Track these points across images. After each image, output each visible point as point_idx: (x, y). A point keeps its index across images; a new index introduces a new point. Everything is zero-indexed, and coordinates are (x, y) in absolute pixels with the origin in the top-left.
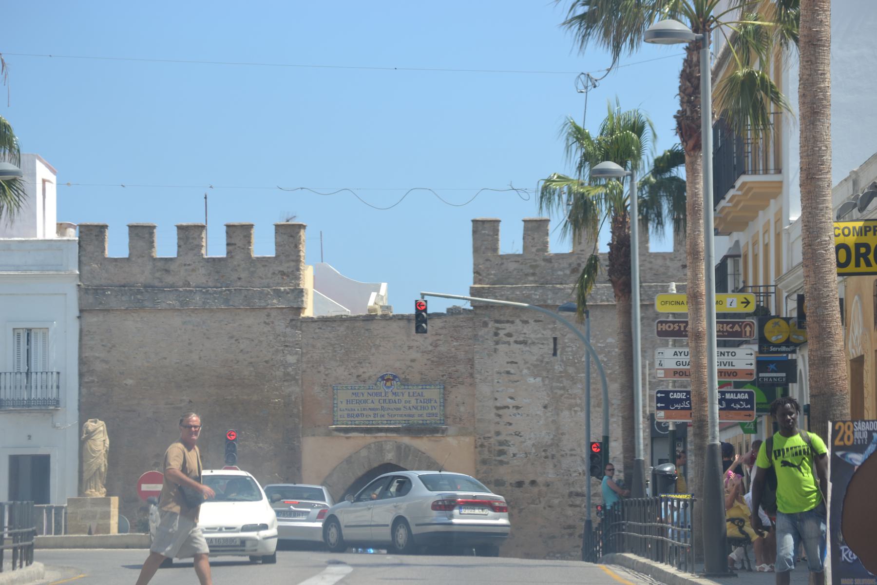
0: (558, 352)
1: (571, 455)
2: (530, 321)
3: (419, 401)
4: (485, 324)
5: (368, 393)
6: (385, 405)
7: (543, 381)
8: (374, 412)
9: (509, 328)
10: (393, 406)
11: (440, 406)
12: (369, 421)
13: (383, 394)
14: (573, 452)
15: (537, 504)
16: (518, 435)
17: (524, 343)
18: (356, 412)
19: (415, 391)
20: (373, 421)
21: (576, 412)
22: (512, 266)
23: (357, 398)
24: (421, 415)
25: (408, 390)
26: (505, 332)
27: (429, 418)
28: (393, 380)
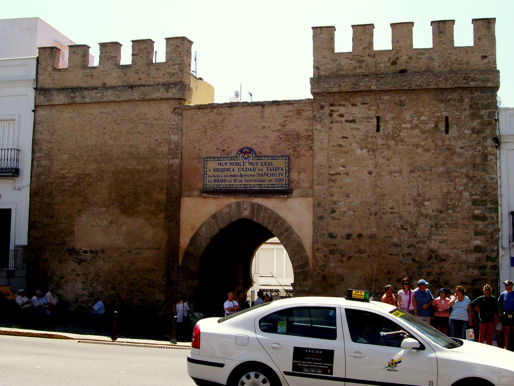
0: (381, 129)
1: (391, 213)
2: (358, 104)
3: (269, 169)
4: (322, 107)
5: (230, 163)
6: (243, 173)
7: (368, 151)
8: (234, 178)
9: (342, 110)
10: (249, 173)
11: (286, 173)
12: (230, 185)
13: (242, 164)
14: (392, 210)
15: (362, 253)
16: (347, 196)
17: (354, 121)
18: (220, 179)
19: (266, 161)
20: (233, 185)
21: (395, 177)
22: (344, 62)
23: (222, 167)
24: (271, 181)
25: (261, 161)
26: (338, 113)
27: (277, 183)
28: (250, 153)
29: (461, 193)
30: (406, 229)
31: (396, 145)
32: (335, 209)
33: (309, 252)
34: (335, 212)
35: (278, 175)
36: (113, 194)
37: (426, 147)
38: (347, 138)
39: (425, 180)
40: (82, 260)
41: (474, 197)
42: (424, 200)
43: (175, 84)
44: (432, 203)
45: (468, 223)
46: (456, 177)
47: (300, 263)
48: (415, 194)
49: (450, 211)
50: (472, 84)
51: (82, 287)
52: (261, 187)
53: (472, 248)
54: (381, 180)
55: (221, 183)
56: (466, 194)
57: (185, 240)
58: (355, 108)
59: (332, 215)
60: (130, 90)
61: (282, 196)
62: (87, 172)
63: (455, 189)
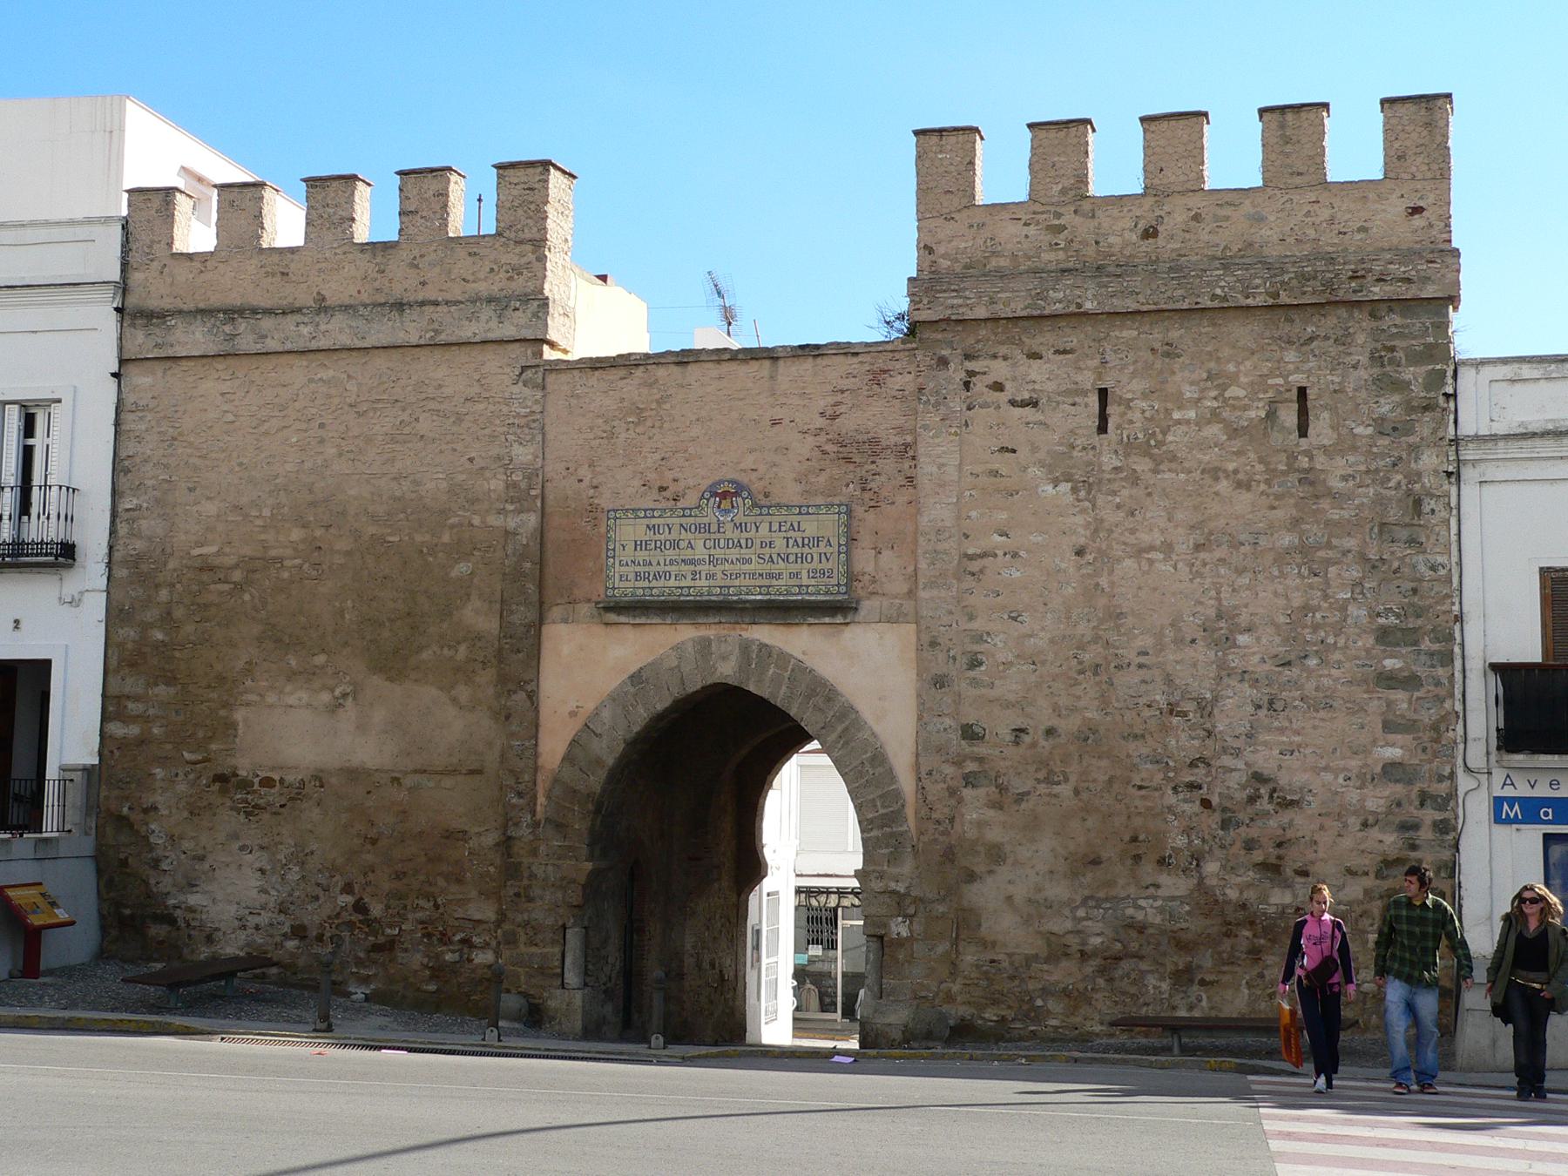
0: (1110, 426)
1: (1140, 666)
2: (1044, 353)
3: (791, 542)
4: (943, 362)
5: (681, 525)
6: (718, 553)
7: (1075, 490)
8: (692, 568)
9: (999, 370)
10: (733, 554)
11: (840, 553)
12: (682, 588)
13: (714, 528)
14: (1142, 659)
15: (1058, 783)
16: (1015, 619)
17: (1033, 403)
18: (652, 569)
19: (782, 518)
20: (689, 588)
21: (1151, 562)
22: (1009, 233)
23: (657, 537)
24: (796, 575)
25: (769, 518)
26: (990, 379)
27: (813, 582)
28: (736, 494)
29: (1343, 609)
30: (1184, 714)
31: (1156, 471)
32: (979, 656)
33: (906, 783)
34: (981, 664)
35: (816, 557)
36: (347, 616)
37: (1241, 476)
38: (1014, 451)
39: (1240, 572)
40: (256, 806)
41: (1382, 621)
42: (1237, 629)
43: (525, 299)
44: (1258, 639)
45: (1365, 696)
46: (1329, 562)
47: (882, 811)
48: (1212, 613)
49: (1312, 662)
50: (1377, 291)
51: (259, 883)
52: (768, 594)
53: (1378, 769)
54: (1111, 572)
55: (654, 584)
56: (1357, 612)
57: (553, 747)
58: (1036, 363)
59: (972, 674)
60: (395, 314)
61: (827, 620)
62: (273, 553)
63: (1326, 597)
